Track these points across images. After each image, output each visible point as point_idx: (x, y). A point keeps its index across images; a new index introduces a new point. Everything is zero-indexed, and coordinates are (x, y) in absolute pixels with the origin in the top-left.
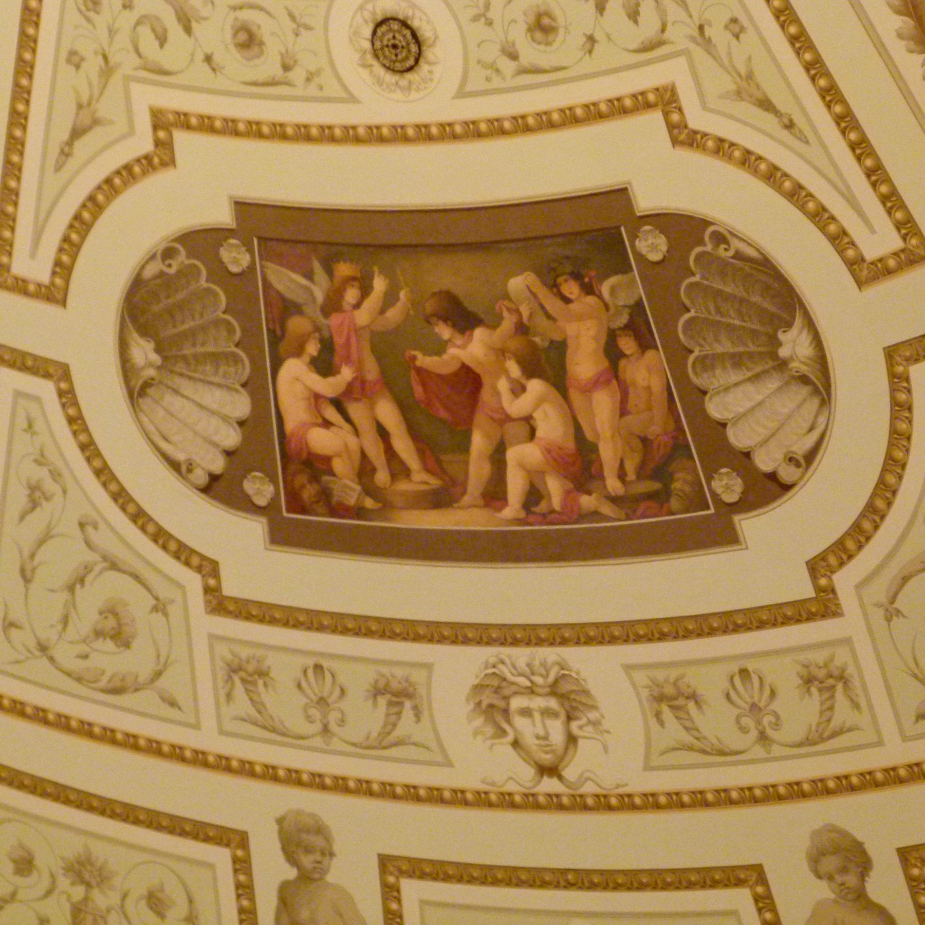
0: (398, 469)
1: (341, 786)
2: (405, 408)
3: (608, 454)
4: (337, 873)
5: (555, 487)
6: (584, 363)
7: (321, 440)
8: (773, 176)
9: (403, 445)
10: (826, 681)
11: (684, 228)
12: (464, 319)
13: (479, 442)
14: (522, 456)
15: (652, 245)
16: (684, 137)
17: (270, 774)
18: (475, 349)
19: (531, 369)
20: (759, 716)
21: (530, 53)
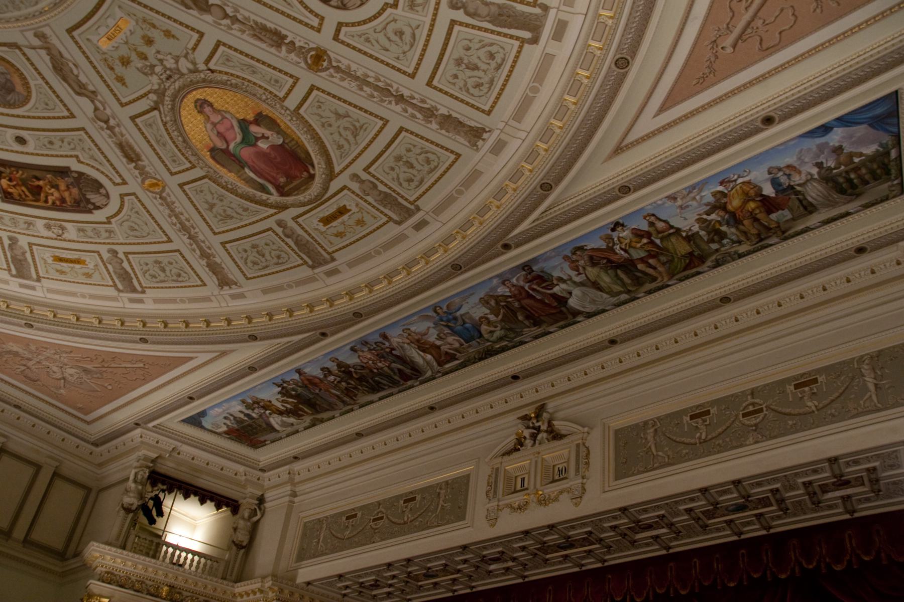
0: (26, 196)
1: (19, 233)
2: (28, 189)
3: (68, 199)
4: (19, 243)
5: (58, 203)
6: (63, 187)
7: (10, 190)
8: (97, 169)
9: (27, 193)
10: (110, 232)
11: (81, 174)
12: (38, 179)
13: (42, 195)
14: (51, 199)
15: (76, 175)
16: (80, 161)
17: (5, 230)
18: (41, 183)
19: (52, 187)
20: (98, 234)
21: (49, 146)
